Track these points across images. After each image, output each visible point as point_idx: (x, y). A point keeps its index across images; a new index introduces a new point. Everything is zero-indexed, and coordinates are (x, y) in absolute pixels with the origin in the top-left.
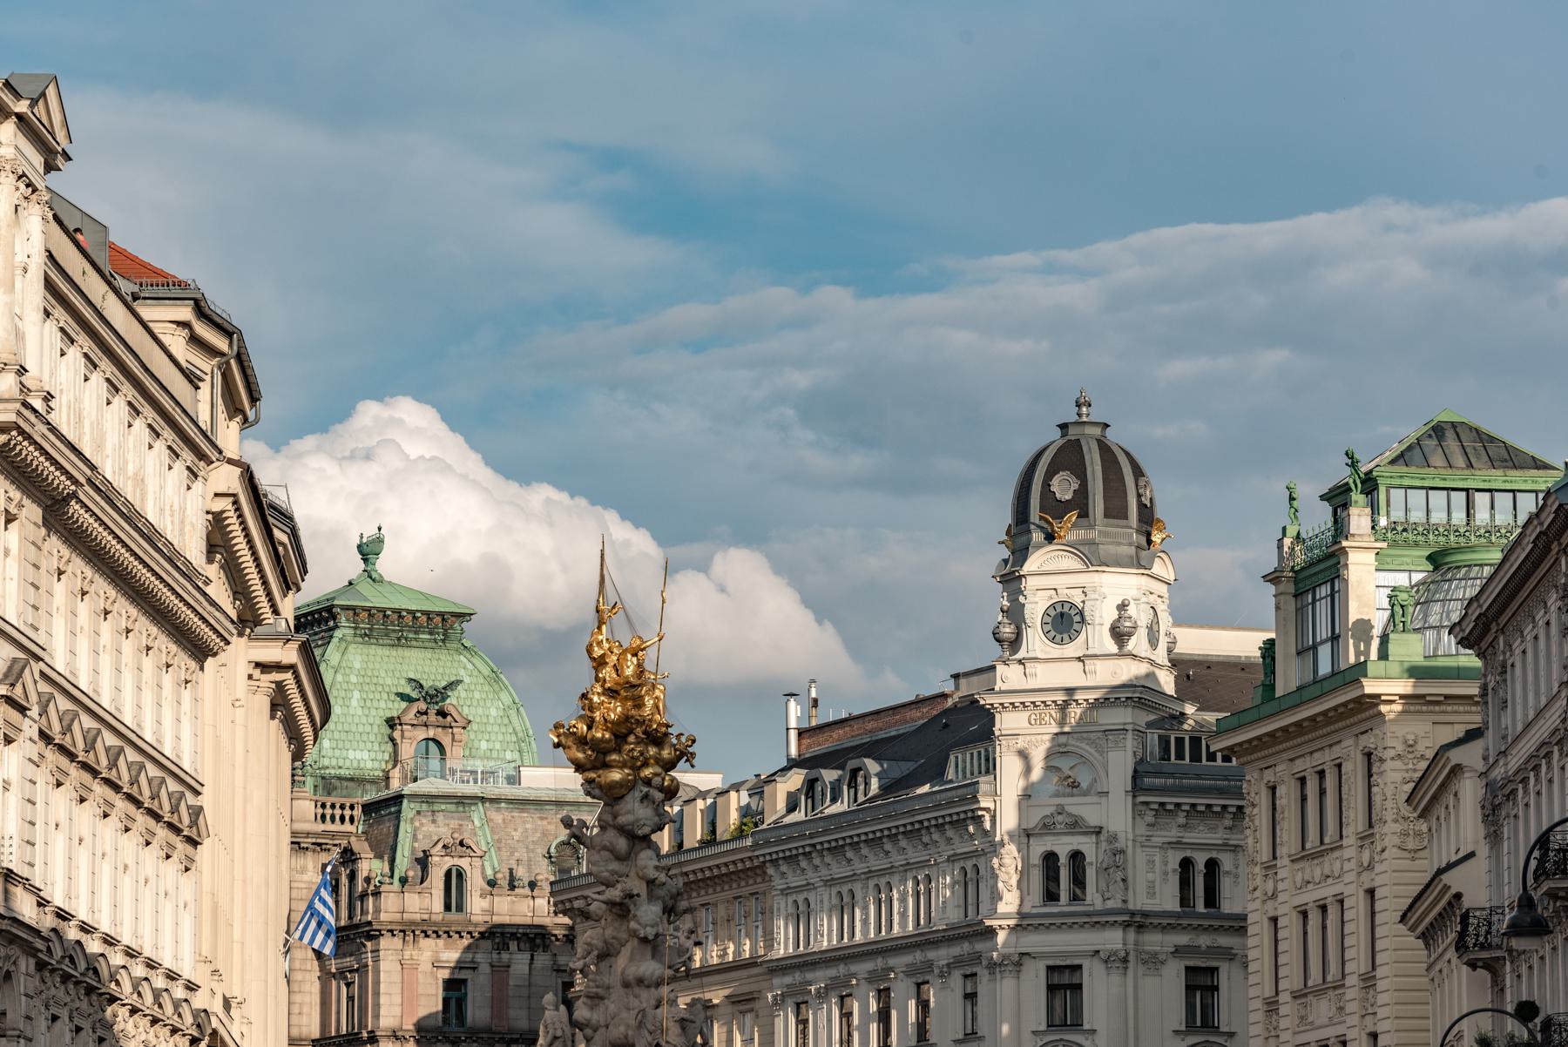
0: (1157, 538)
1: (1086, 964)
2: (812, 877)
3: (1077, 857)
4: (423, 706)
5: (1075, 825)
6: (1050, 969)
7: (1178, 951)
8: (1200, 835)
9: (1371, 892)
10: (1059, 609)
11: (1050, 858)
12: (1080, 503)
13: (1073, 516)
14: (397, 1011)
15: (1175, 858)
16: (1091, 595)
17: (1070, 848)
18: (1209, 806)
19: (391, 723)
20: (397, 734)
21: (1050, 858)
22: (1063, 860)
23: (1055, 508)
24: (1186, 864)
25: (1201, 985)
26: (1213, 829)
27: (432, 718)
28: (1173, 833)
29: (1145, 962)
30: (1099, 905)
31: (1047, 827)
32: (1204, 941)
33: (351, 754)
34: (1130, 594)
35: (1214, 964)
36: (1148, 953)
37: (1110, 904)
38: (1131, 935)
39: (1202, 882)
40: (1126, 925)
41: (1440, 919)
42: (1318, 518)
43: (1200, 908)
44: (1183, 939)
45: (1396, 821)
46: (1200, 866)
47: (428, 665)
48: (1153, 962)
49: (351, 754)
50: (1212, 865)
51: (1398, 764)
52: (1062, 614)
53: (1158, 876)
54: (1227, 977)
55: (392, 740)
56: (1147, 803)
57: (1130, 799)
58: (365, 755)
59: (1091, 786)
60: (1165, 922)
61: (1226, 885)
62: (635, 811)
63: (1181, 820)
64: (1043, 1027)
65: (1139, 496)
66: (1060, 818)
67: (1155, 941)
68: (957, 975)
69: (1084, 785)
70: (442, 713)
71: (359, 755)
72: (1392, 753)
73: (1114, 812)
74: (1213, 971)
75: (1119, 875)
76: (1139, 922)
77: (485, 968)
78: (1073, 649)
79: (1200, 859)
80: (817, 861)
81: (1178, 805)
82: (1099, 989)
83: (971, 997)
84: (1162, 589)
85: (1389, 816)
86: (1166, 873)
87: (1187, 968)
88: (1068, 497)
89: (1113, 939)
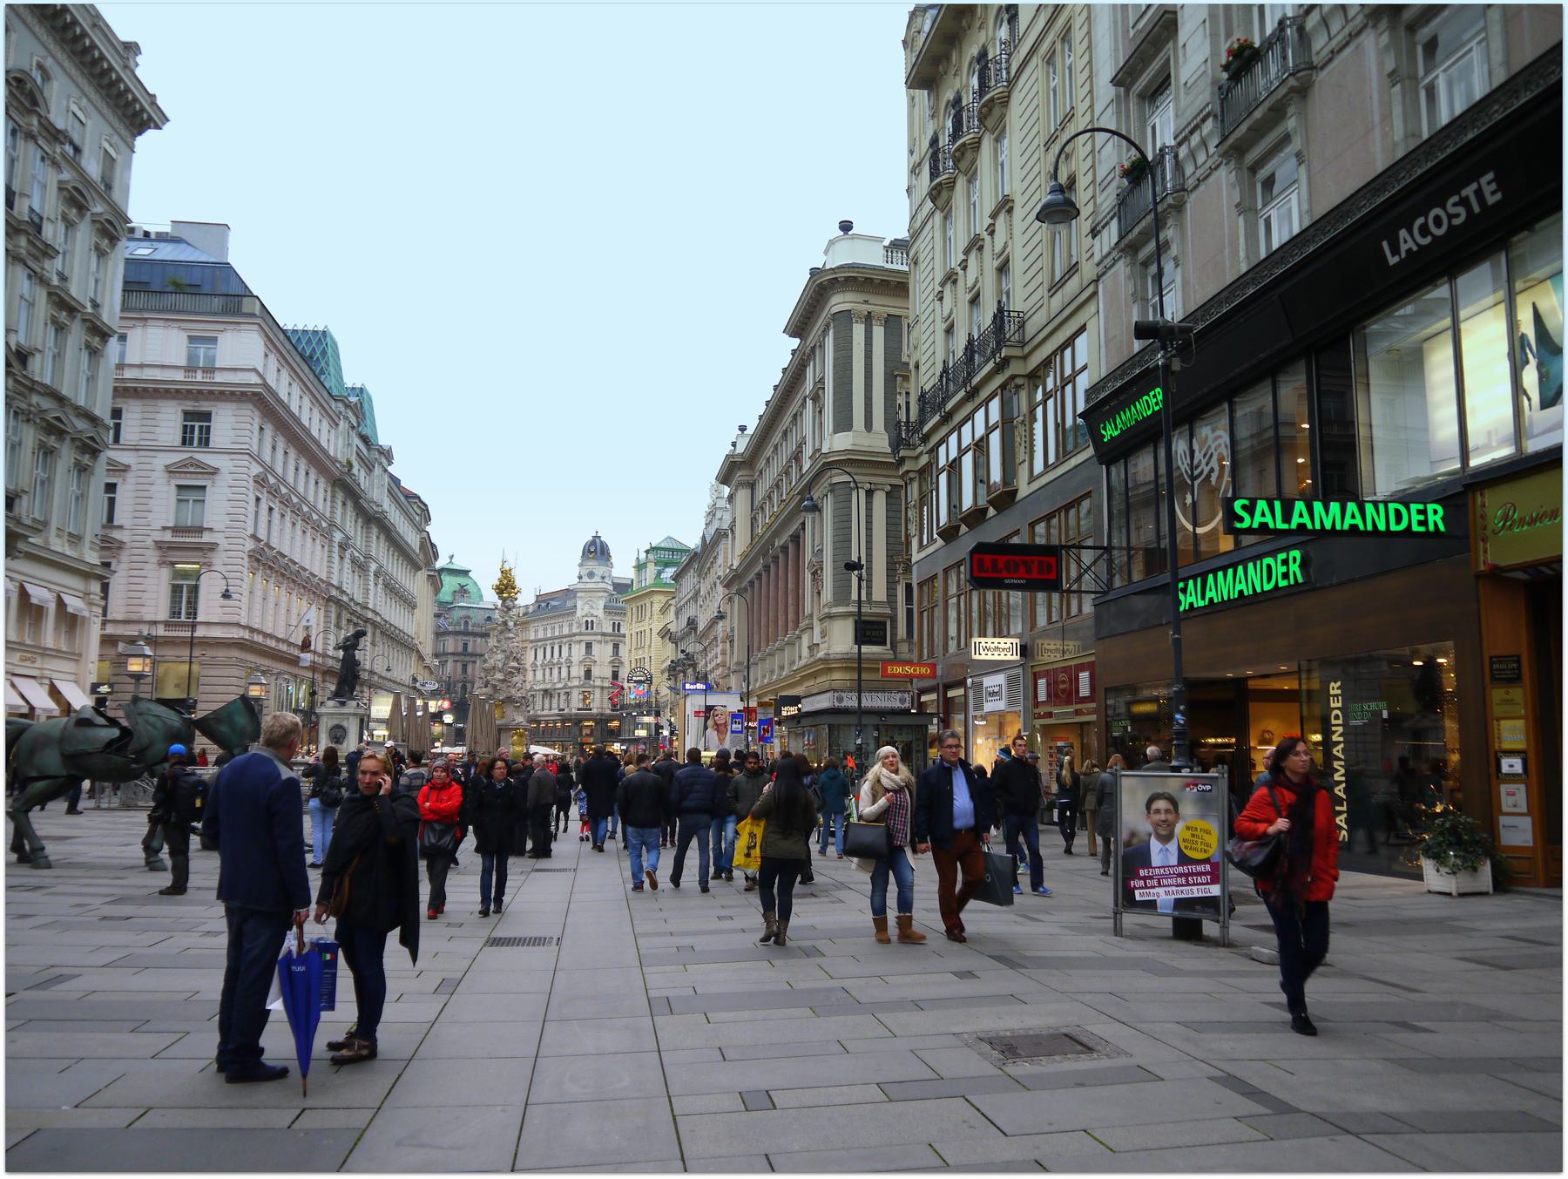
41: (665, 634)
42: (643, 556)
47: (462, 580)
62: (509, 603)
73: (600, 613)
76: (604, 634)
82: (596, 648)
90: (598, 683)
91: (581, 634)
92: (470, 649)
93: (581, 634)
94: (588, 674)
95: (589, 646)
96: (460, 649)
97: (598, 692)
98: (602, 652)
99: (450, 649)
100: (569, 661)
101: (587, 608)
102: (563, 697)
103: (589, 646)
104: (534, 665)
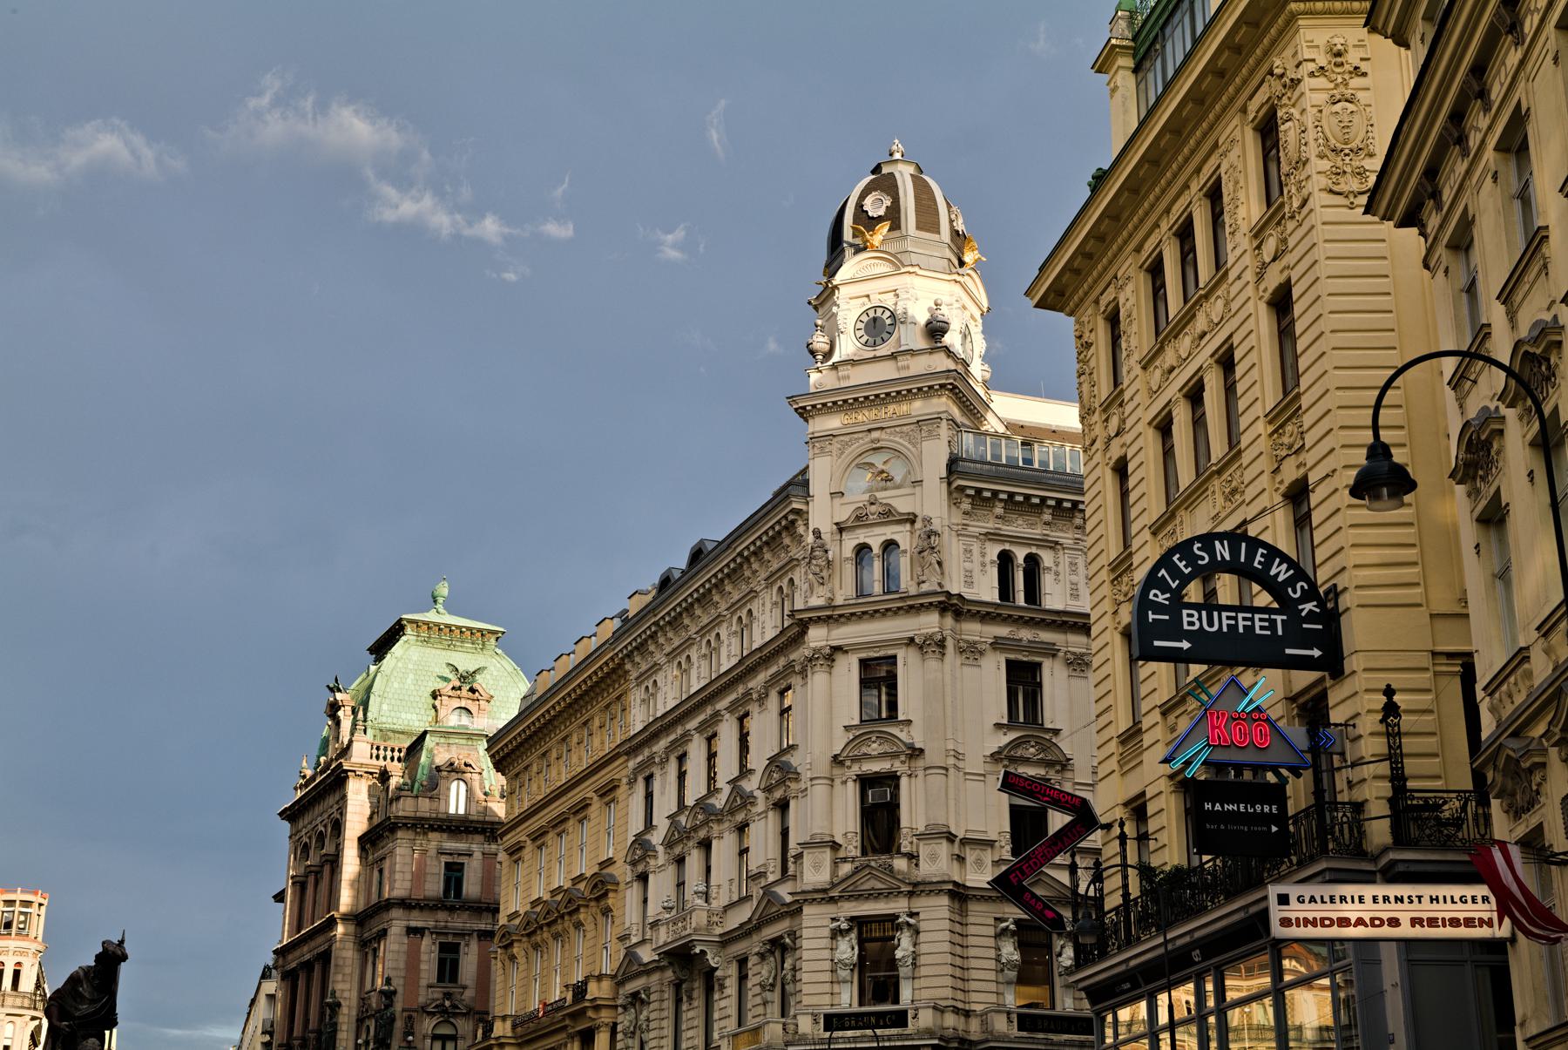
0: (969, 257)
1: (901, 654)
2: (660, 658)
3: (890, 546)
4: (458, 684)
5: (889, 516)
6: (864, 663)
7: (998, 644)
8: (1019, 527)
9: (1281, 303)
10: (871, 313)
11: (862, 550)
12: (893, 216)
13: (884, 228)
14: (408, 885)
15: (993, 551)
16: (902, 296)
17: (883, 538)
18: (1027, 497)
19: (434, 695)
20: (437, 703)
21: (862, 550)
22: (876, 550)
23: (866, 222)
24: (1005, 560)
25: (1024, 680)
26: (1032, 525)
27: (464, 692)
28: (990, 525)
29: (962, 652)
30: (913, 591)
31: (860, 520)
32: (1025, 634)
33: (403, 716)
34: (945, 299)
35: (1037, 659)
36: (967, 641)
37: (925, 588)
38: (949, 621)
39: (1020, 575)
40: (943, 608)
43: (1020, 599)
44: (1003, 631)
45: (1321, 156)
46: (1020, 559)
48: (971, 651)
49: (403, 716)
50: (1032, 562)
51: (1321, 82)
52: (875, 319)
53: (976, 567)
54: (1053, 677)
55: (434, 707)
56: (961, 489)
57: (945, 485)
58: (414, 717)
59: (905, 478)
60: (984, 609)
61: (1048, 582)
63: (999, 510)
64: (856, 722)
65: (951, 221)
66: (873, 508)
67: (973, 630)
68: (773, 702)
69: (898, 479)
70: (472, 690)
71: (409, 716)
72: (1311, 67)
73: (933, 502)
74: (1039, 665)
75: (933, 559)
76: (954, 607)
77: (478, 855)
78: (884, 350)
79: (1020, 554)
80: (661, 640)
81: (995, 493)
82: (911, 674)
83: (784, 712)
84: (977, 314)
85: (1312, 151)
86: (983, 565)
87: (1008, 662)
88: (881, 212)
89: (930, 623)
90: (936, 863)
91: (831, 616)
92: (471, 887)
93: (831, 616)
94: (880, 821)
95: (878, 676)
96: (434, 886)
97: (935, 912)
98: (954, 704)
99: (399, 885)
100: (781, 768)
101: (859, 487)
102: (760, 972)
103: (878, 676)
104: (641, 844)
